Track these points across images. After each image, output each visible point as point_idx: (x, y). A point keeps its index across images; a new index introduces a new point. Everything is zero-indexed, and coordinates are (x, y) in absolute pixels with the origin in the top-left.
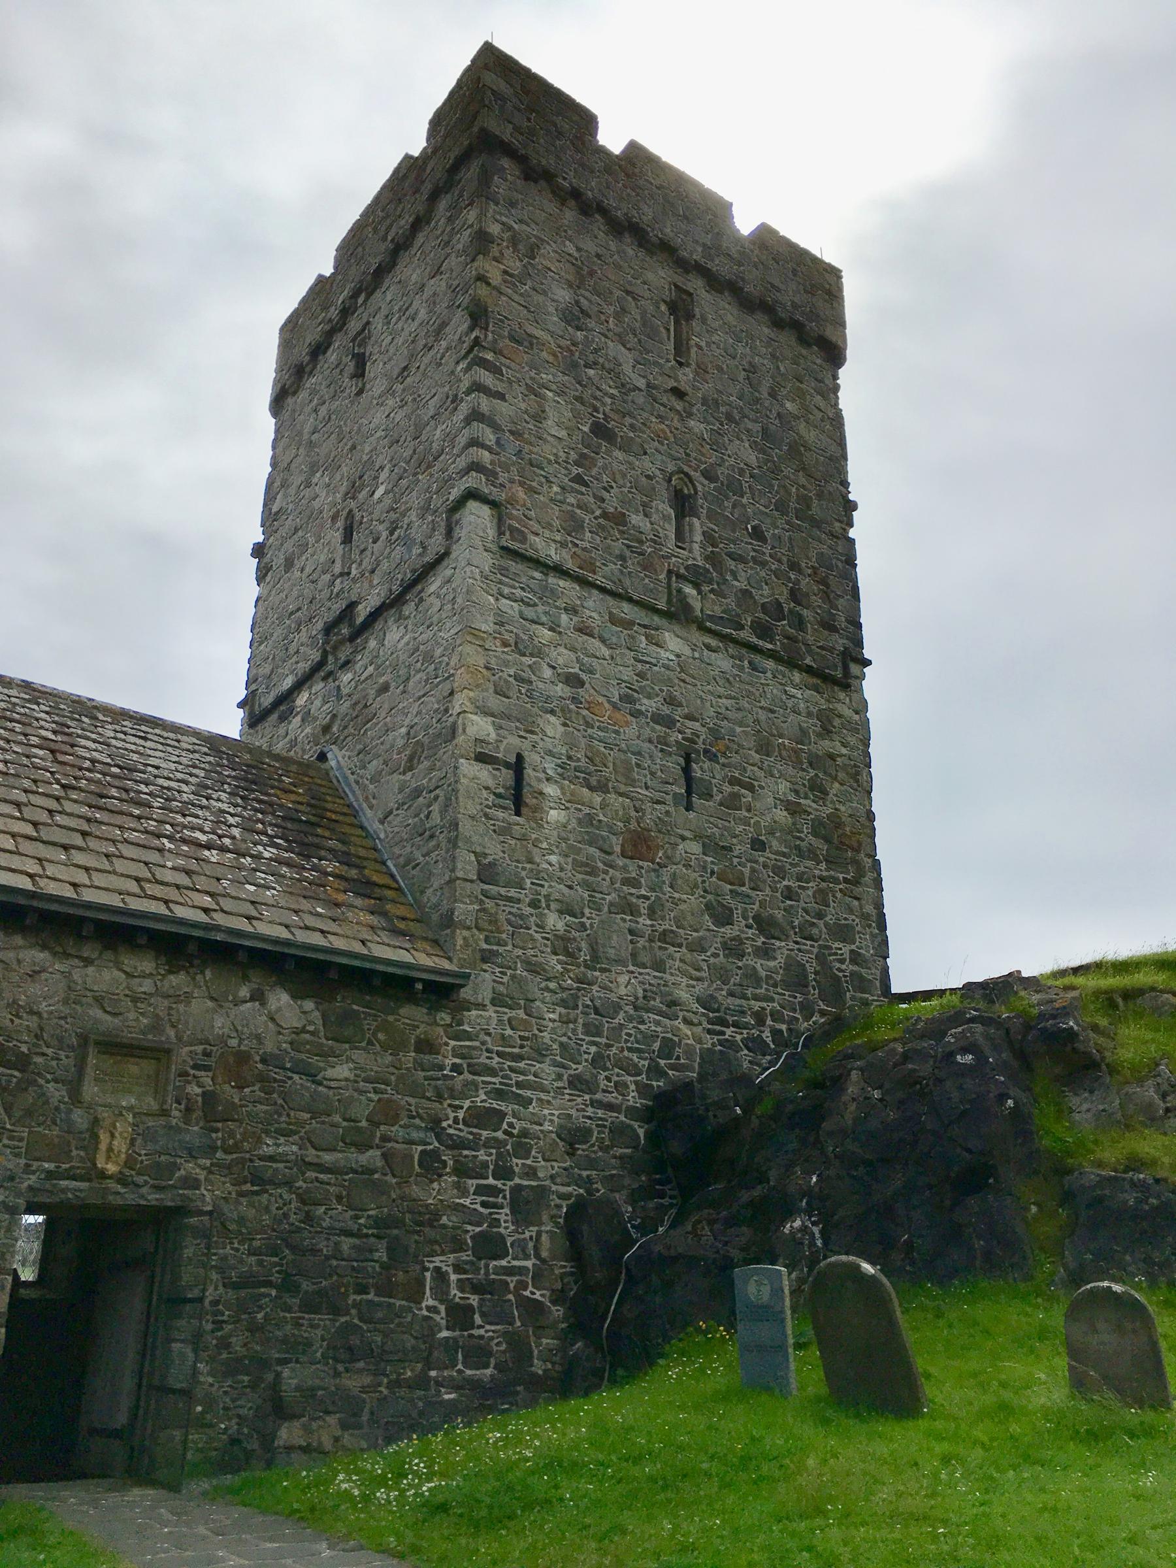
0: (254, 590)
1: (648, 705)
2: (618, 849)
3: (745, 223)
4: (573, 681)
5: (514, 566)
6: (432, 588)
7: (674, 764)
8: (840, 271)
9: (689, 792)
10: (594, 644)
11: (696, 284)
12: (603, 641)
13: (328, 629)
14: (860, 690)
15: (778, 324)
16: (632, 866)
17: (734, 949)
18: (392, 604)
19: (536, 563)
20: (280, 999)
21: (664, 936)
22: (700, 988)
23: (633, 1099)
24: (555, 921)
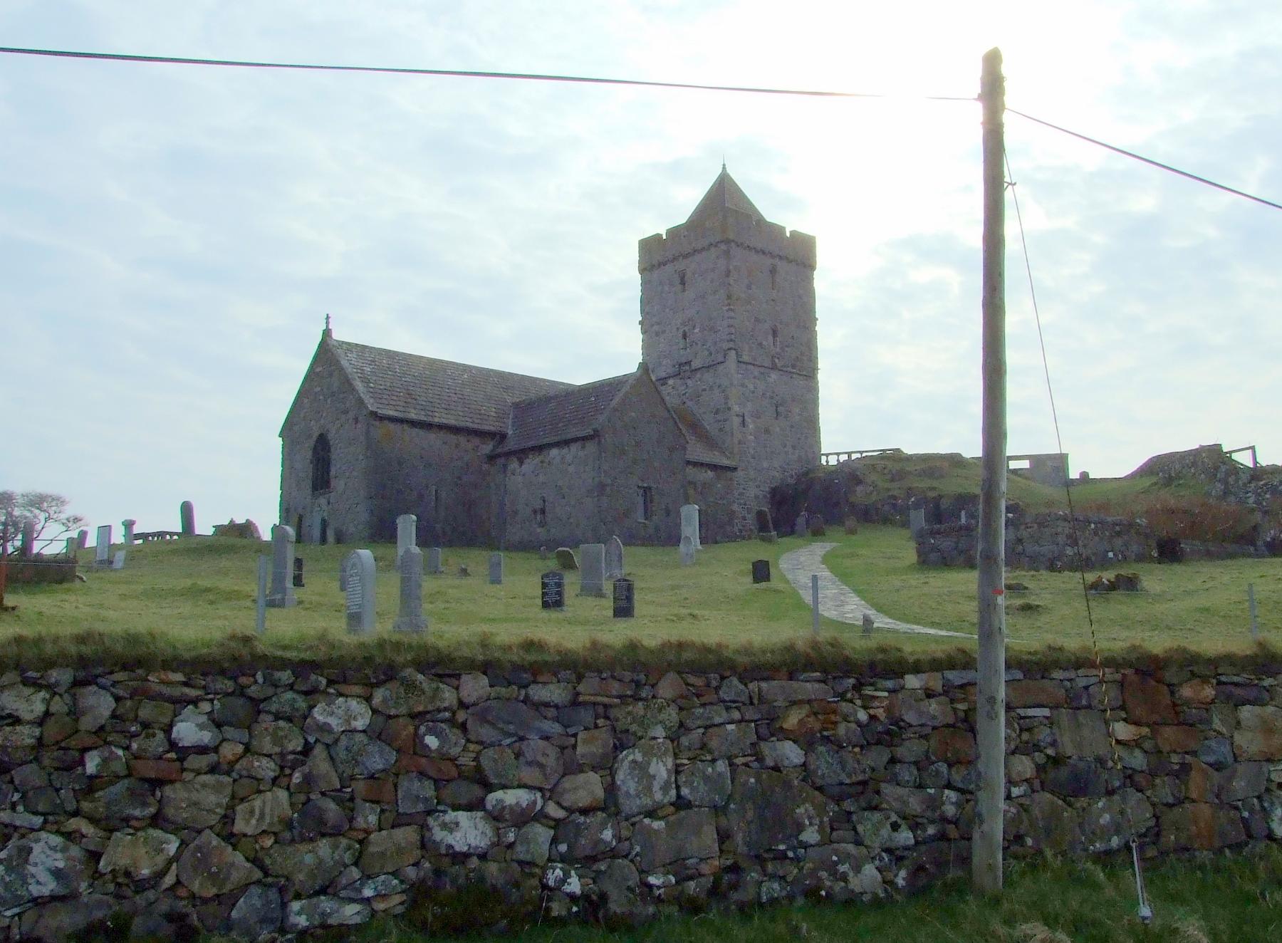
0: (641, 336)
4: (753, 392)
11: (777, 261)
19: (744, 363)
20: (709, 472)
23: (767, 489)
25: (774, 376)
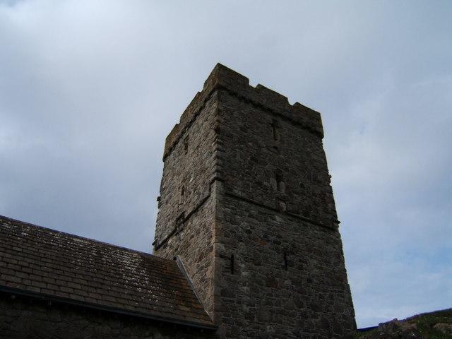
1: (272, 238)
2: (265, 284)
3: (292, 102)
5: (229, 199)
6: (206, 206)
7: (281, 256)
8: (319, 114)
9: (286, 265)
10: (255, 221)
11: (279, 119)
12: (257, 219)
13: (178, 219)
14: (337, 231)
15: (304, 128)
16: (270, 289)
17: (304, 315)
18: (195, 211)
21: (282, 313)
22: (294, 329)
24: (246, 308)
25: (278, 219)
